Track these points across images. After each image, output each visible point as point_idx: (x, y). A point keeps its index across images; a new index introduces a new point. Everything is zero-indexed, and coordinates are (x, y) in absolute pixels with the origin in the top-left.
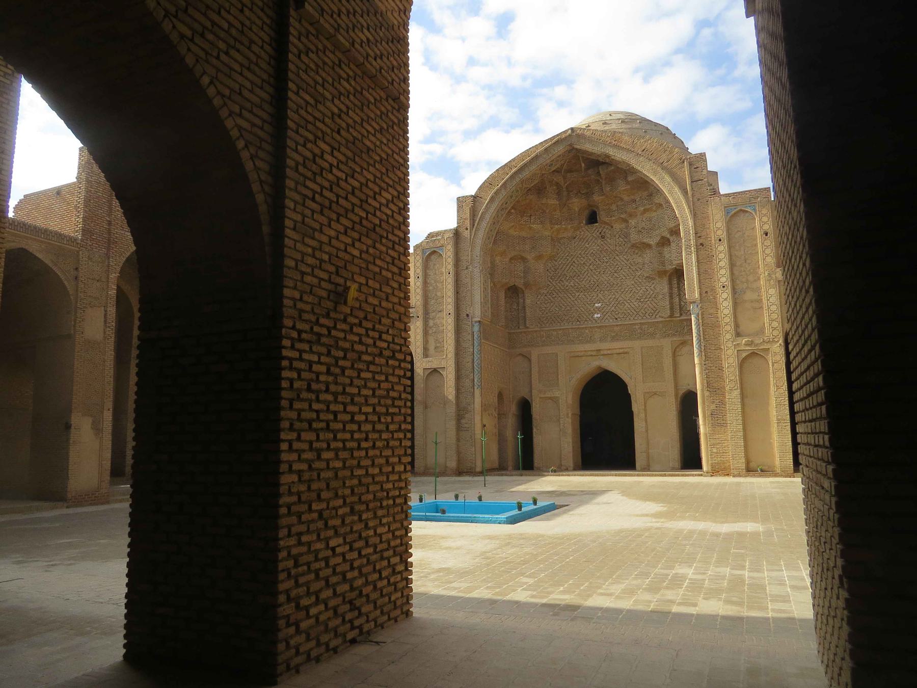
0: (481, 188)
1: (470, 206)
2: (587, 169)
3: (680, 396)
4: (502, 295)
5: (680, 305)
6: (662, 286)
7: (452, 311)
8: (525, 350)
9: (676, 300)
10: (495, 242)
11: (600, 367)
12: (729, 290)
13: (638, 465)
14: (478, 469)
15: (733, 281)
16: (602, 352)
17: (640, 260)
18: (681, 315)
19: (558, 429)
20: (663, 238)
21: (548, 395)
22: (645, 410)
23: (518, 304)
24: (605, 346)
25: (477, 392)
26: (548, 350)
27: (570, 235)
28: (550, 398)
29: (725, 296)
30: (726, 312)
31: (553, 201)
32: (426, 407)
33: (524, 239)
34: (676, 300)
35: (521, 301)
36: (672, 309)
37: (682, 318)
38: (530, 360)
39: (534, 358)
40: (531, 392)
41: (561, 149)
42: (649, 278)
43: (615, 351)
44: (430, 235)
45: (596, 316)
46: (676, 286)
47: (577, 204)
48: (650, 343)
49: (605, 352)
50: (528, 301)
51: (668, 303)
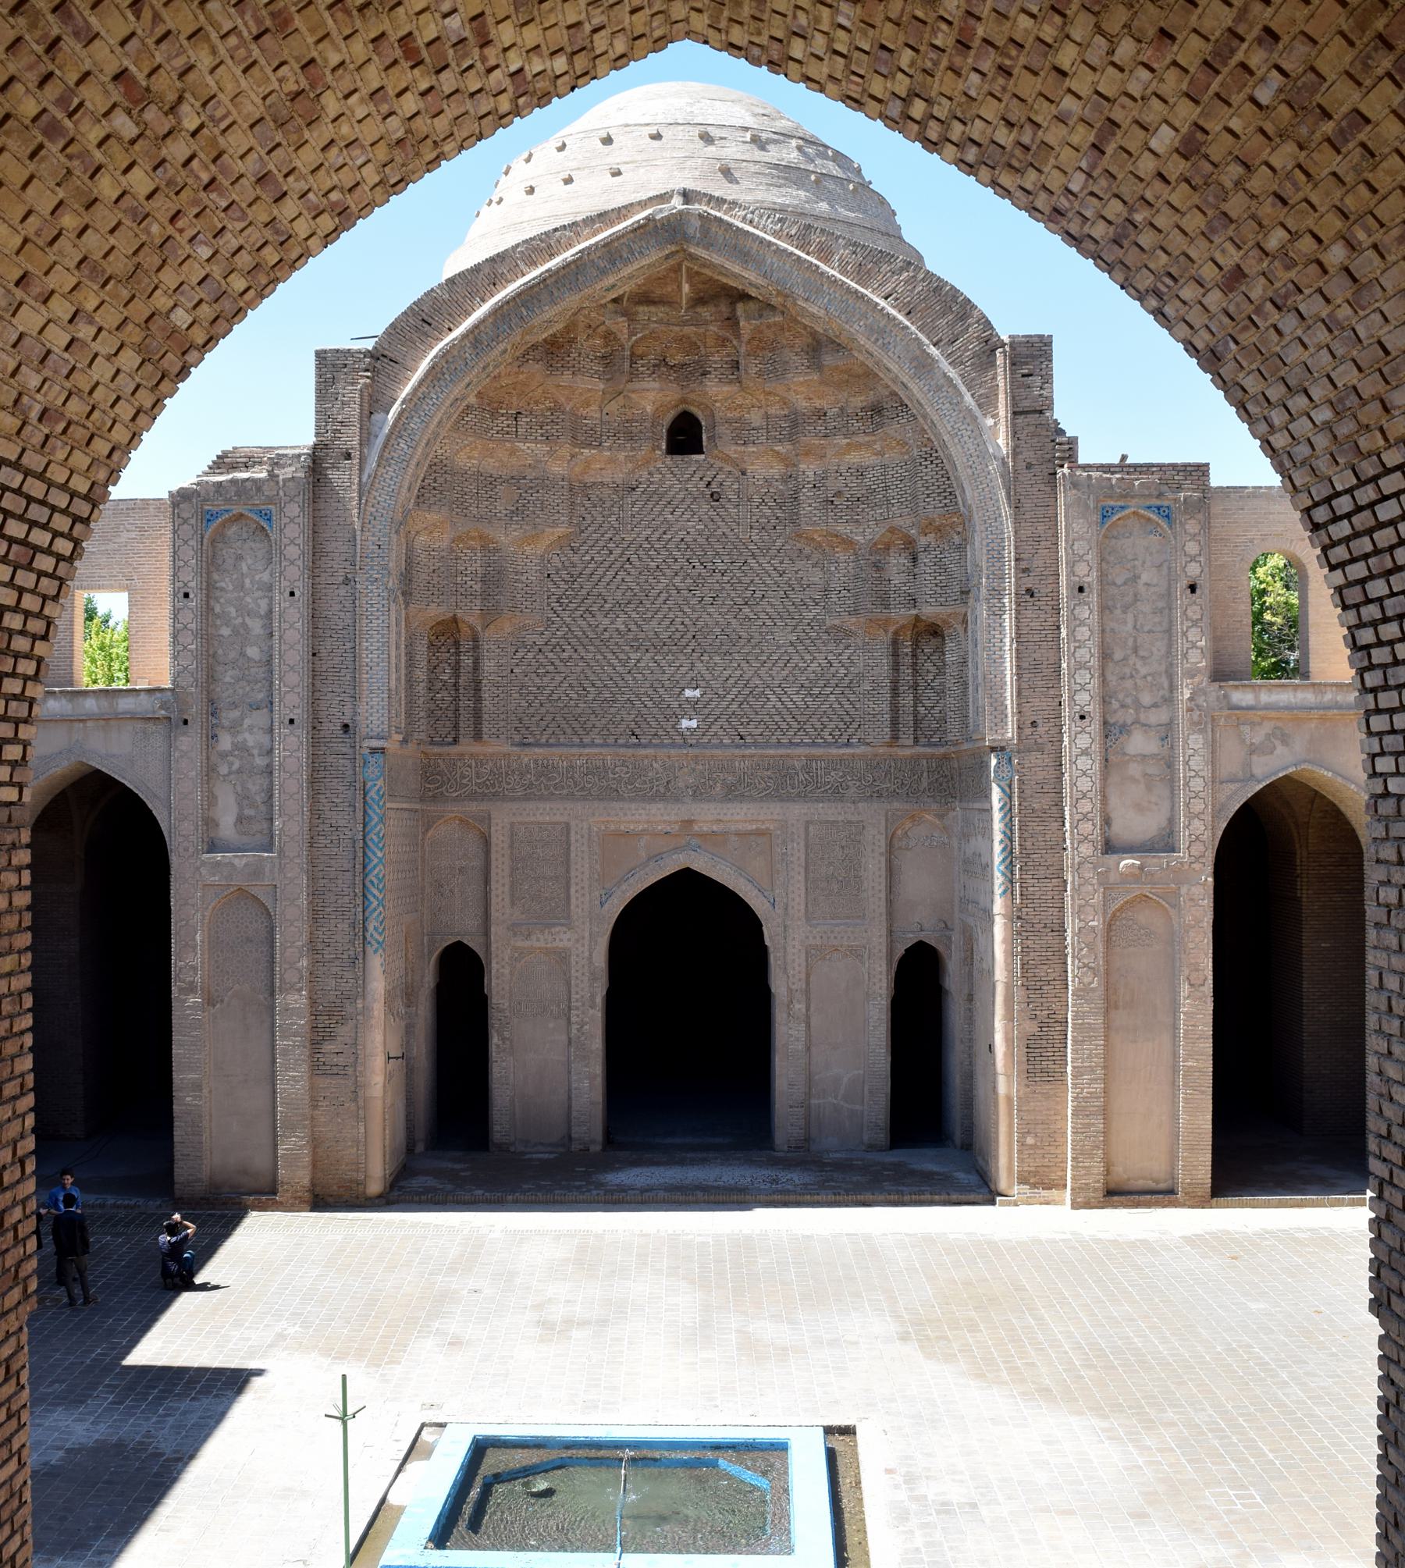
2: (699, 301)
3: (900, 951)
5: (916, 714)
7: (298, 714)
8: (473, 807)
9: (907, 700)
12: (1094, 727)
14: (375, 1187)
15: (1105, 701)
17: (816, 577)
18: (916, 740)
20: (892, 530)
22: (807, 992)
24: (708, 815)
27: (619, 477)
29: (1083, 741)
31: (590, 385)
33: (492, 481)
34: (907, 700)
35: (467, 661)
36: (895, 723)
38: (486, 842)
45: (685, 723)
46: (908, 660)
48: (829, 811)
50: (488, 666)
51: (885, 707)
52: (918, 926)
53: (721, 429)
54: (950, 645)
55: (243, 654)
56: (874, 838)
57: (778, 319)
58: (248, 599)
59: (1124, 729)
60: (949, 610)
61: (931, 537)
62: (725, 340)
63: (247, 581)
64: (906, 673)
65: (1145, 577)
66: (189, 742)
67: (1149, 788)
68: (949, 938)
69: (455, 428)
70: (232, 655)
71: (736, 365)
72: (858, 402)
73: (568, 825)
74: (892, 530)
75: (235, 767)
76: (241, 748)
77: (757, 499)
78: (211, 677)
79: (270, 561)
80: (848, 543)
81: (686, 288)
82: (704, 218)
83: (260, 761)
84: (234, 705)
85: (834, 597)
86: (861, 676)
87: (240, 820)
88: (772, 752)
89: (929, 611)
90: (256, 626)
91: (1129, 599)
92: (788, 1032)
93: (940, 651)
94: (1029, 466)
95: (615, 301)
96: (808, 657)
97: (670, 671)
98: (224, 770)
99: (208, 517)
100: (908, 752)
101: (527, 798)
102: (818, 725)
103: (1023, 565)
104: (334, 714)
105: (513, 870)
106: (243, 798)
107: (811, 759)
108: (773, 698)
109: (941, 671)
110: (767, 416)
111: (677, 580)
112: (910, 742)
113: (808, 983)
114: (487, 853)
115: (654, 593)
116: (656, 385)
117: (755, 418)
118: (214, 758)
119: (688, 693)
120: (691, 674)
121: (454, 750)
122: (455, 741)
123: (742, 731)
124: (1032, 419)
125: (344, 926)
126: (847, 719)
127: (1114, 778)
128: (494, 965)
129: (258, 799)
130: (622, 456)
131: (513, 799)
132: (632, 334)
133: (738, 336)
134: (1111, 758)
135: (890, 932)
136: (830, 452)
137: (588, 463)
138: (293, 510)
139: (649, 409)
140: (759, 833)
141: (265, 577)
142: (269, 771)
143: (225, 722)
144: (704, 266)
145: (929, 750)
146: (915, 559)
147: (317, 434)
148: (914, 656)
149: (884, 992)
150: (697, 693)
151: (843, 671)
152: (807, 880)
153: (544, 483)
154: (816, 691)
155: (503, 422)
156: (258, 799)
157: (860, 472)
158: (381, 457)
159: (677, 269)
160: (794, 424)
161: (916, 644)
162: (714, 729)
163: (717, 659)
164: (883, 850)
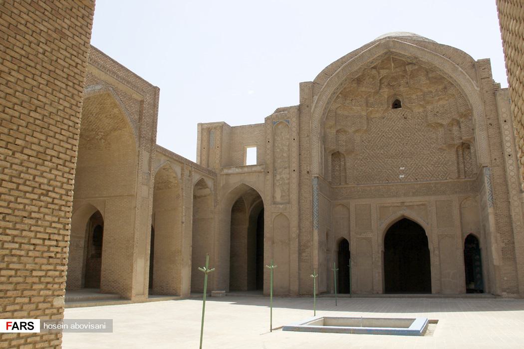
0: (319, 77)
3: (465, 236)
4: (330, 158)
6: (451, 156)
9: (462, 166)
11: (403, 216)
16: (405, 204)
18: (465, 177)
19: (369, 262)
20: (453, 120)
24: (408, 200)
25: (316, 233)
32: (273, 243)
33: (347, 117)
34: (462, 166)
35: (343, 163)
36: (459, 172)
37: (466, 179)
38: (349, 209)
39: (352, 209)
42: (441, 150)
43: (415, 204)
44: (278, 111)
45: (401, 176)
47: (386, 92)
49: (408, 204)
50: (348, 164)
51: (456, 168)
52: (471, 229)
54: (472, 148)
55: (282, 155)
57: (417, 67)
58: (284, 142)
60: (470, 137)
62: (404, 76)
63: (284, 138)
66: (269, 177)
68: (480, 232)
69: (335, 101)
71: (407, 83)
72: (441, 87)
75: (281, 182)
76: (282, 179)
77: (416, 118)
78: (274, 162)
79: (289, 133)
80: (442, 125)
81: (393, 65)
82: (393, 41)
83: (287, 182)
85: (439, 141)
87: (281, 197)
88: (425, 182)
90: (286, 149)
92: (434, 260)
93: (470, 152)
94: (487, 92)
96: (433, 157)
97: (396, 163)
99: (274, 123)
100: (463, 180)
102: (437, 175)
103: (487, 117)
104: (305, 168)
107: (436, 183)
108: (424, 168)
110: (417, 95)
112: (464, 177)
113: (439, 245)
115: (390, 143)
116: (387, 90)
117: (414, 97)
118: (275, 181)
119: (401, 168)
120: (402, 163)
121: (341, 186)
124: (486, 80)
126: (445, 173)
128: (352, 243)
129: (286, 191)
132: (379, 77)
133: (407, 75)
135: (462, 231)
137: (371, 112)
138: (294, 119)
139: (386, 97)
140: (423, 205)
141: (288, 137)
142: (289, 184)
143: (278, 172)
145: (469, 179)
146: (460, 127)
148: (463, 154)
149: (461, 247)
150: (403, 168)
151: (443, 160)
152: (437, 217)
154: (436, 166)
161: (463, 151)
162: (409, 177)
163: (408, 159)
164: (458, 207)
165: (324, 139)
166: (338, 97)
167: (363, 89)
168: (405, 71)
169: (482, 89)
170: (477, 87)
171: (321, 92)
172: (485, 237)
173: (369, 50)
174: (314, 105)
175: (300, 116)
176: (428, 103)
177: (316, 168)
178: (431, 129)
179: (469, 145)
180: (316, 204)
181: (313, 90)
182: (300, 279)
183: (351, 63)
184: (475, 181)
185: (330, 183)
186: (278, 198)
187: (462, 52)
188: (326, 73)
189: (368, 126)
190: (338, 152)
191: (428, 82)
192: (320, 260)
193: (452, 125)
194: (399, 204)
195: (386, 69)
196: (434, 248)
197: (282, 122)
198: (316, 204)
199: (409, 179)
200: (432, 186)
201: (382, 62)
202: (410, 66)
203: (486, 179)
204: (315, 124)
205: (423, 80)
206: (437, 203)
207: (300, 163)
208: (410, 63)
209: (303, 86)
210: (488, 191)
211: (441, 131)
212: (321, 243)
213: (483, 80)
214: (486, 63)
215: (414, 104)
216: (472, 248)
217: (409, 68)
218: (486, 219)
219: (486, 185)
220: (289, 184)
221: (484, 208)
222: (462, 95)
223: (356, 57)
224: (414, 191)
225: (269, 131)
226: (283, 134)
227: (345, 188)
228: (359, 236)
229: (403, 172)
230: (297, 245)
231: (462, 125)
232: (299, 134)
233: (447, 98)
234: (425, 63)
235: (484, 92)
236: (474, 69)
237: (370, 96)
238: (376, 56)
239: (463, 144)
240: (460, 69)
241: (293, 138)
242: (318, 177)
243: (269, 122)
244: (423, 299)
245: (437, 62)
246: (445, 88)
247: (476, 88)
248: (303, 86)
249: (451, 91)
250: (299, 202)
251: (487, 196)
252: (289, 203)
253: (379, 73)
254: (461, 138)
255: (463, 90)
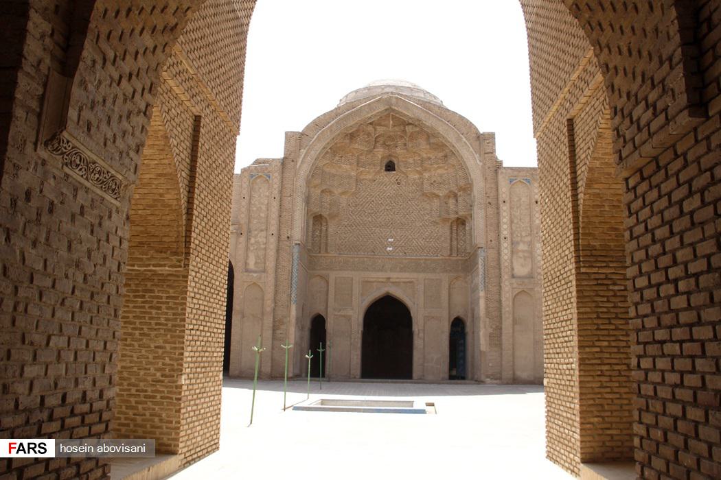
0: (308, 127)
1: (295, 141)
5: (457, 247)
6: (444, 231)
10: (313, 176)
11: (388, 293)
13: (415, 375)
15: (512, 234)
16: (391, 280)
17: (428, 207)
19: (346, 343)
20: (450, 192)
21: (342, 313)
22: (424, 330)
23: (321, 231)
26: (345, 274)
28: (344, 316)
29: (505, 245)
30: (506, 257)
32: (243, 317)
33: (334, 176)
34: (455, 243)
35: (324, 228)
36: (451, 250)
37: (458, 258)
38: (327, 282)
39: (332, 282)
40: (327, 308)
41: (382, 108)
44: (257, 162)
45: (388, 249)
46: (455, 231)
47: (380, 153)
49: (394, 280)
51: (449, 245)
52: (458, 312)
53: (400, 163)
54: (467, 224)
56: (445, 285)
59: (518, 243)
60: (466, 213)
61: (461, 193)
63: (262, 195)
64: (454, 235)
65: (523, 199)
66: (242, 239)
67: (525, 260)
70: (256, 215)
71: (405, 145)
72: (441, 154)
73: (352, 279)
74: (450, 192)
75: (255, 247)
76: (257, 242)
78: (249, 222)
80: (437, 196)
82: (397, 98)
83: (263, 246)
84: (256, 230)
86: (441, 236)
87: (256, 263)
89: (461, 213)
90: (264, 208)
91: (518, 205)
92: (418, 343)
93: (464, 229)
94: (489, 168)
95: (370, 124)
98: (252, 248)
99: (252, 176)
101: (340, 270)
105: (335, 292)
106: (257, 257)
107: (426, 260)
109: (465, 235)
110: (414, 160)
111: (387, 207)
114: (328, 286)
116: (382, 150)
117: (411, 160)
118: (249, 245)
119: (390, 240)
121: (320, 255)
122: (320, 252)
123: (406, 251)
125: (285, 296)
127: (515, 257)
129: (261, 257)
130: (372, 171)
131: (337, 270)
133: (406, 135)
134: (514, 250)
135: (449, 313)
136: (432, 170)
138: (276, 174)
139: (380, 157)
141: (267, 194)
142: (265, 249)
144: (396, 114)
145: (460, 258)
146: (457, 201)
147: (285, 154)
148: (457, 230)
153: (350, 177)
155: (337, 158)
156: (261, 257)
157: (441, 176)
158: (302, 161)
159: (389, 115)
160: (422, 161)
164: (447, 287)
165: (308, 200)
166: (327, 153)
167: (356, 146)
168: (404, 131)
169: (485, 164)
170: (480, 161)
171: (311, 145)
172: (473, 321)
173: (369, 104)
174: (301, 159)
175: (283, 173)
176: (426, 170)
177: (297, 234)
178: (426, 199)
179: (464, 221)
180: (295, 274)
181: (300, 142)
182: (272, 360)
183: (348, 115)
184: (466, 260)
185: (309, 250)
186: (252, 266)
187: (468, 121)
188: (317, 124)
189: (356, 187)
190: (320, 215)
191: (428, 147)
192: (293, 337)
193: (449, 197)
194: (385, 280)
195: (384, 126)
196: (419, 330)
197: (261, 176)
198: (295, 274)
199: (398, 252)
200: (422, 262)
201: (381, 117)
202: (410, 126)
203: (480, 261)
204: (301, 182)
205: (423, 145)
206: (426, 281)
207: (279, 226)
208: (411, 124)
209: (289, 136)
210: (481, 273)
211: (436, 202)
212: (297, 319)
213: (486, 155)
214: (491, 136)
215: (410, 169)
216: (458, 330)
217: (409, 129)
218: (475, 302)
219: (480, 267)
220: (265, 249)
221: (474, 290)
222: (463, 167)
223: (353, 110)
224: (402, 266)
225: (245, 186)
226: (261, 190)
227: (324, 257)
228: (336, 313)
229: (391, 244)
230: (272, 320)
231: (460, 199)
232: (281, 192)
233: (446, 168)
234: (428, 127)
235: (487, 168)
236: (478, 142)
237: (361, 155)
238: (374, 113)
239: (458, 219)
240: (464, 139)
241: (273, 196)
242: (299, 244)
243: (246, 174)
244: (408, 385)
245: (441, 129)
246: (446, 156)
247: (478, 161)
248: (289, 136)
249: (452, 161)
250: (276, 271)
251: (480, 279)
252: (264, 271)
253: (375, 130)
254: (457, 213)
255: (465, 162)
